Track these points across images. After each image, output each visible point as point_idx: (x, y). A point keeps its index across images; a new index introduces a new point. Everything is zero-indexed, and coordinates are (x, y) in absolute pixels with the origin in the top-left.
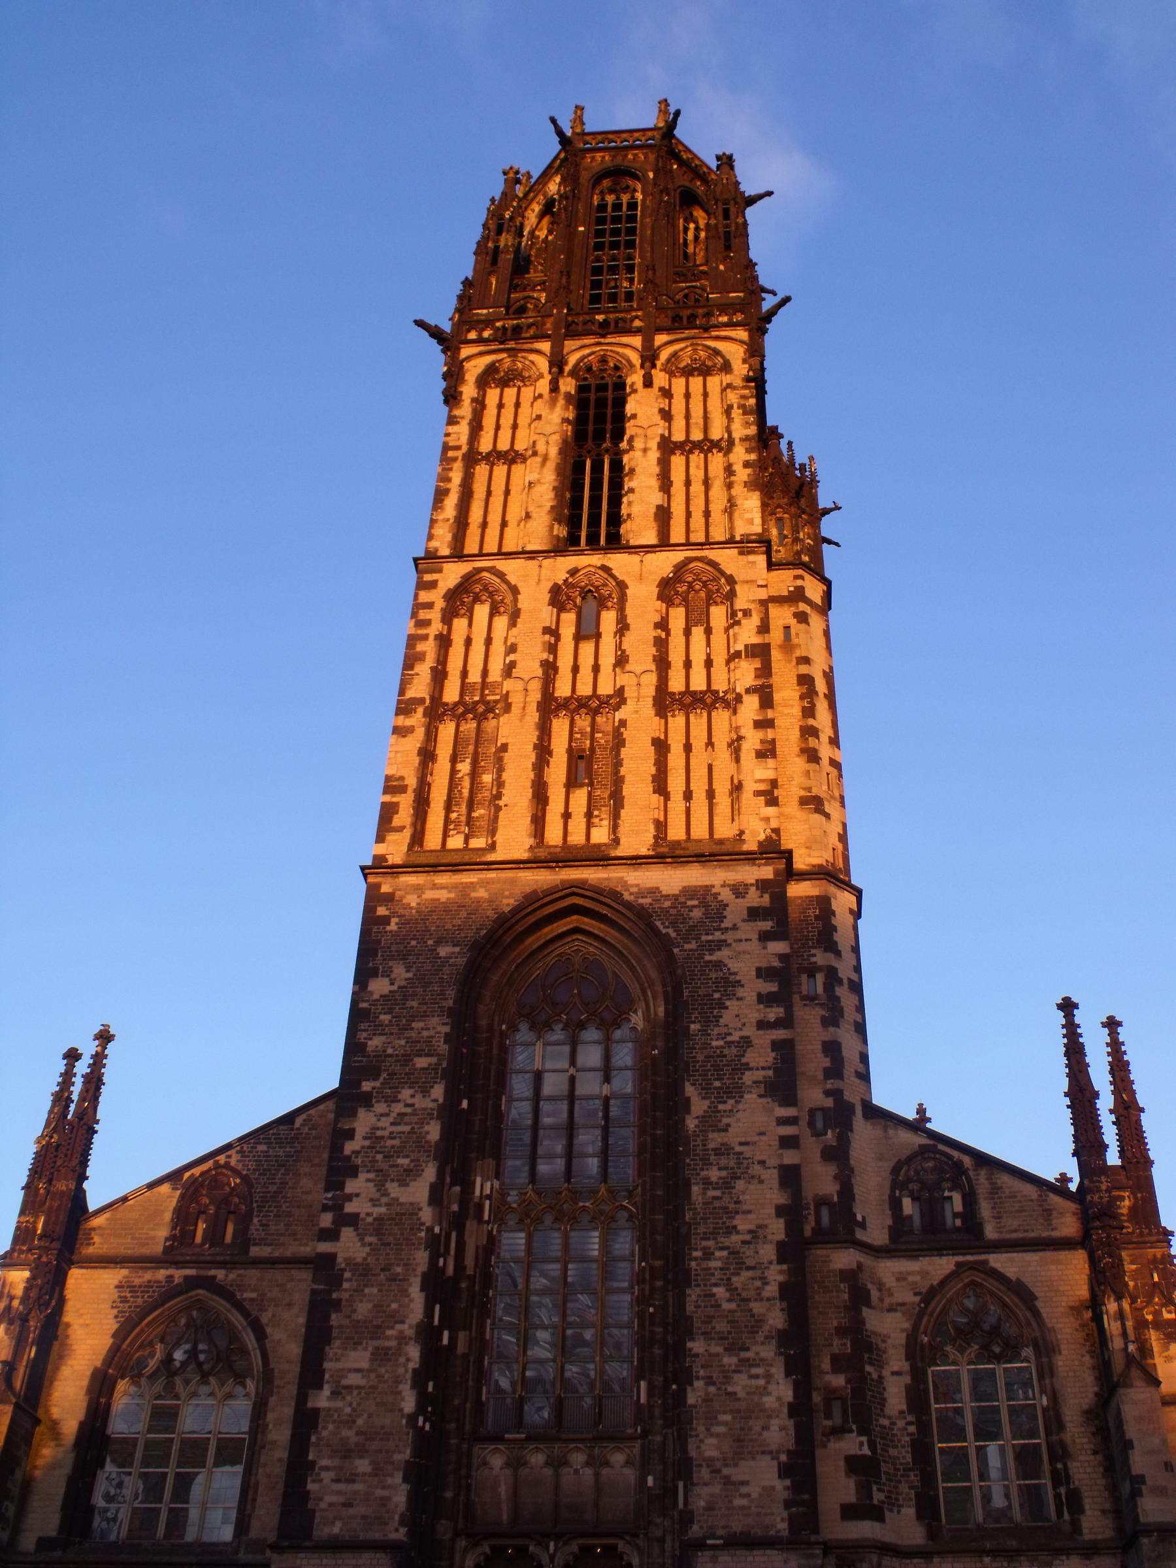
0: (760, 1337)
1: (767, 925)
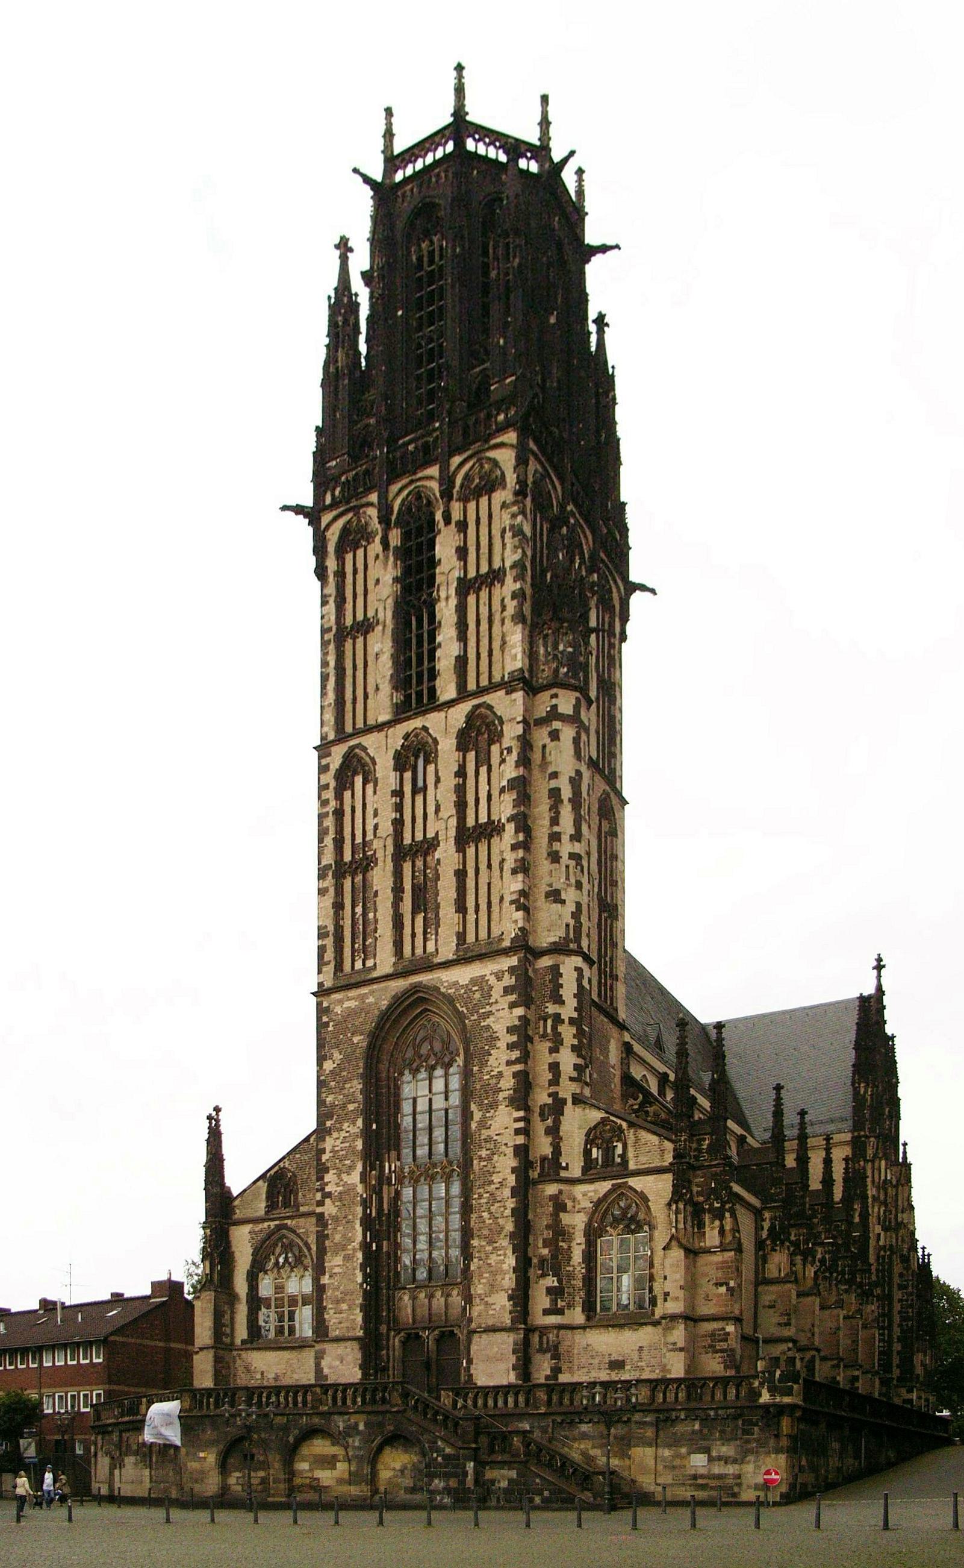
0: (502, 1236)
1: (513, 998)
